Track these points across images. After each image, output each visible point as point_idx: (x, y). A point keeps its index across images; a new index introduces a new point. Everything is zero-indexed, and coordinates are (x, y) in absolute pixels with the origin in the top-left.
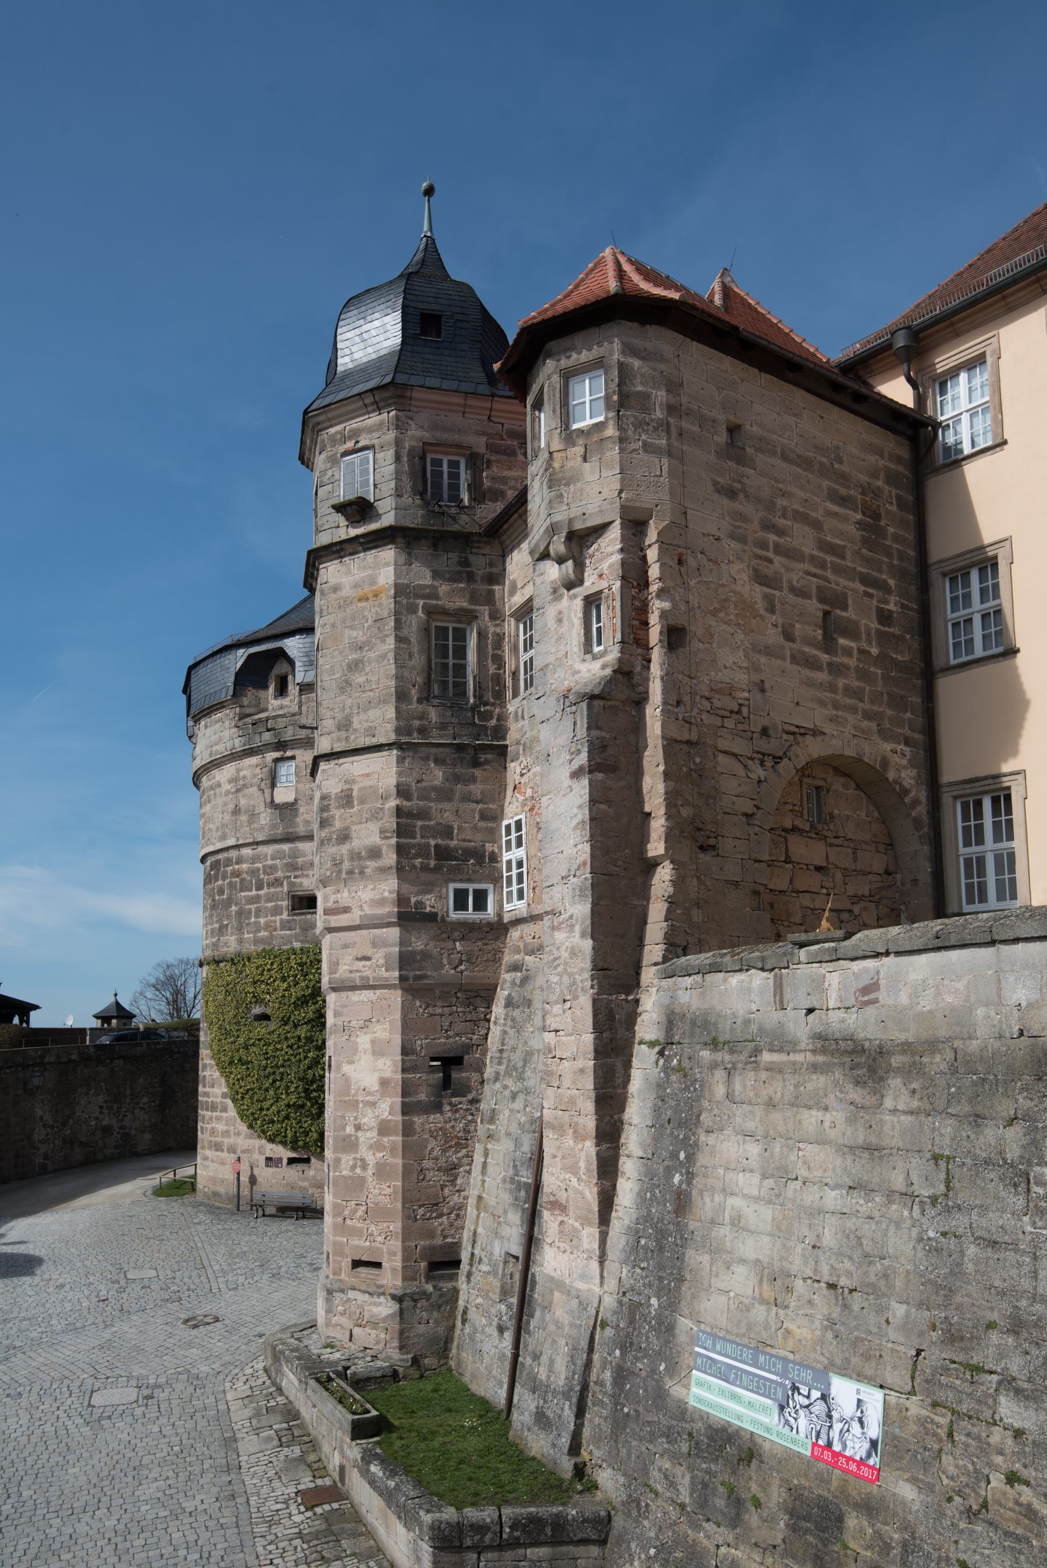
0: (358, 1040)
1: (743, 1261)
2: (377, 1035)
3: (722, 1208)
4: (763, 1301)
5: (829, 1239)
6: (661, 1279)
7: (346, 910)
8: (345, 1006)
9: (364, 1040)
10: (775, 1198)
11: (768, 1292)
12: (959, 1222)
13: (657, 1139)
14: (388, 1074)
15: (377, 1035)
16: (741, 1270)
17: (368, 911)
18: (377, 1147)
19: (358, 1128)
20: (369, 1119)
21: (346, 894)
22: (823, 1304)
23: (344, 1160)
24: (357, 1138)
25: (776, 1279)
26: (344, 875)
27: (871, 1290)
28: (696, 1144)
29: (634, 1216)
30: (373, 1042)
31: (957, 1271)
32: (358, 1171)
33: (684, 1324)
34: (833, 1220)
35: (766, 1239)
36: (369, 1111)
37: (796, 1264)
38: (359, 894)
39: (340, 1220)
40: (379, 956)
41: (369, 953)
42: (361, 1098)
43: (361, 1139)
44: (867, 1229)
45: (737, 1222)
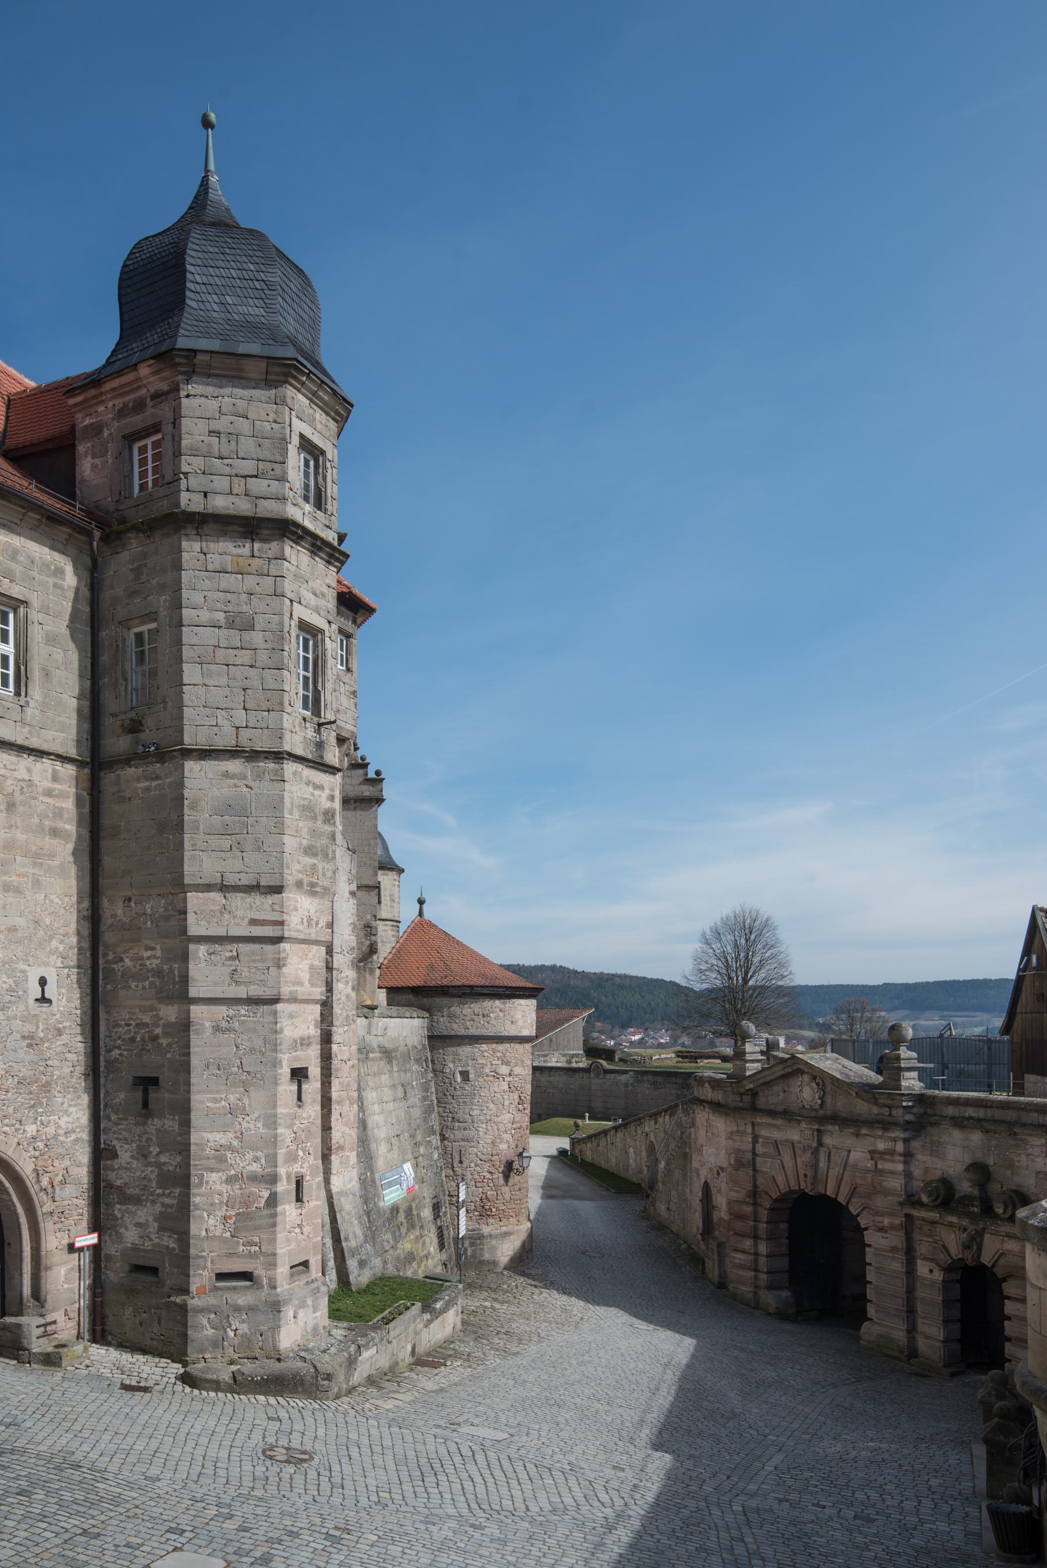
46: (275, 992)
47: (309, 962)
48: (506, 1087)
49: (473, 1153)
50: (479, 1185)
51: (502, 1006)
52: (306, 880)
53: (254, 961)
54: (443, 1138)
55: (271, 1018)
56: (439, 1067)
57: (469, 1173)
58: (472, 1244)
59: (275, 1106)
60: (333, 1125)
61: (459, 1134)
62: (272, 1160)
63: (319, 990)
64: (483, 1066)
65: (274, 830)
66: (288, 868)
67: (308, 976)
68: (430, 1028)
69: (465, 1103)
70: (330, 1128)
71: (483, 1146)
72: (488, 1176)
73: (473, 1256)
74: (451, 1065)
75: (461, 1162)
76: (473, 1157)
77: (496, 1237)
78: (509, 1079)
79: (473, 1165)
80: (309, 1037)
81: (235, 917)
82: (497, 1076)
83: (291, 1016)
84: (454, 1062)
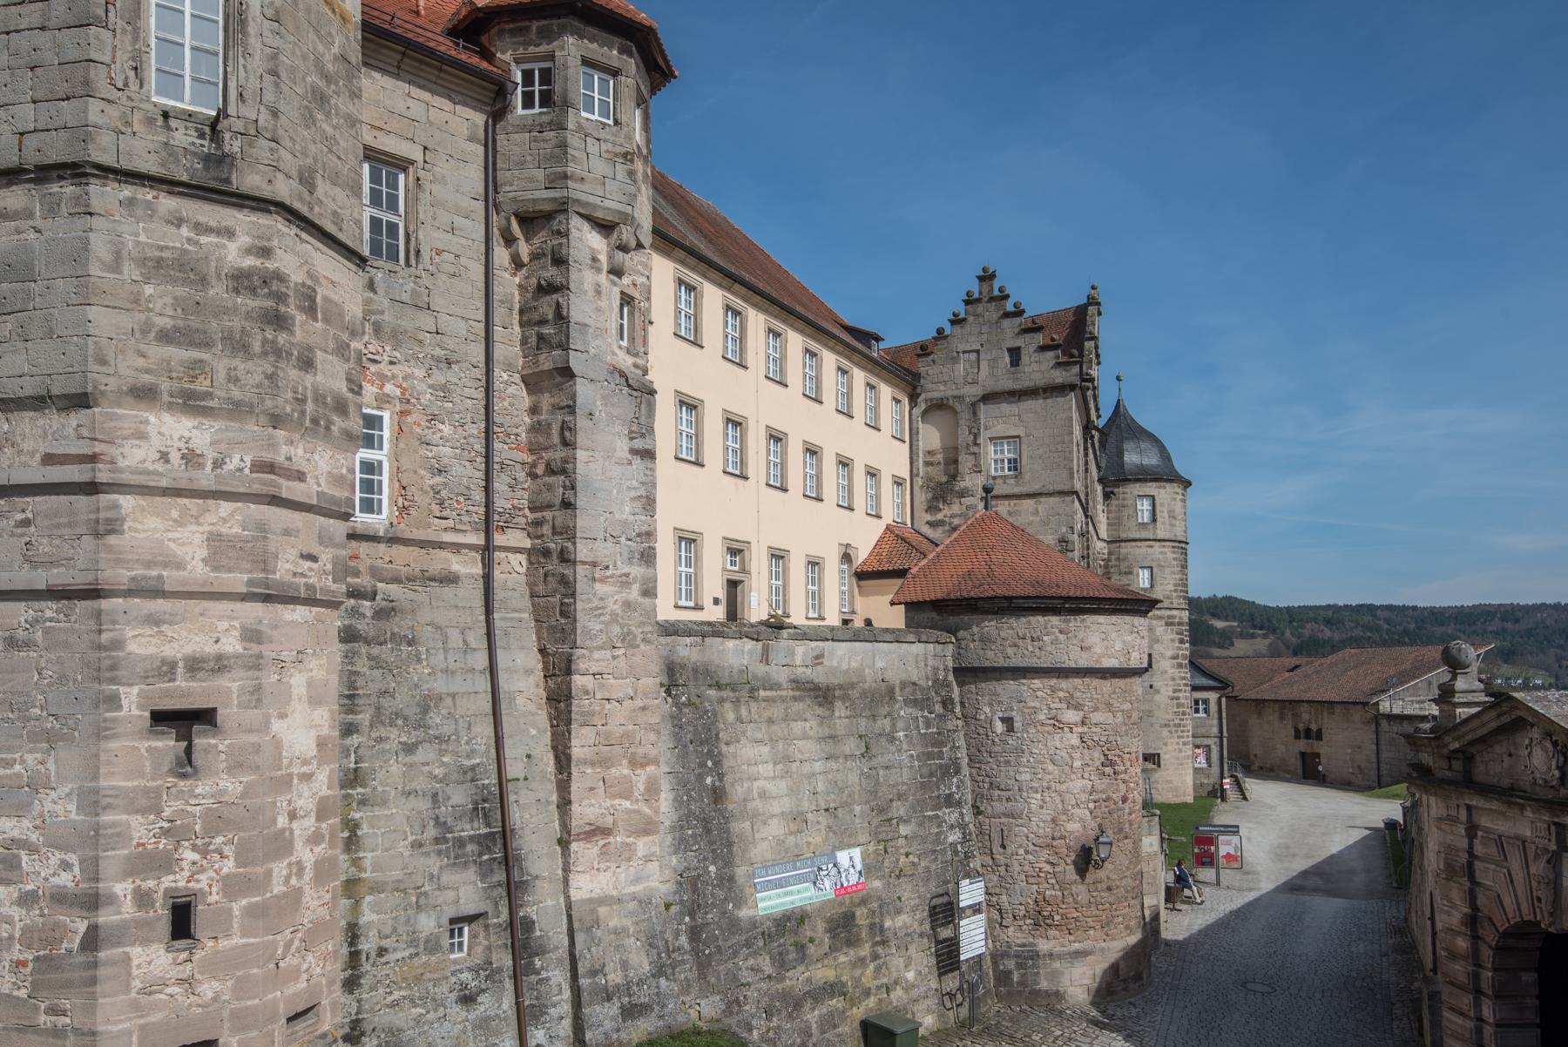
0: (292, 681)
1: (773, 816)
2: (314, 673)
3: (750, 790)
4: (791, 833)
5: (821, 787)
6: (714, 851)
7: (300, 476)
8: (276, 627)
9: (298, 682)
10: (786, 774)
11: (793, 827)
12: (875, 762)
13: (683, 756)
14: (326, 731)
15: (314, 673)
16: (775, 821)
17: (325, 488)
18: (315, 839)
19: (293, 816)
20: (304, 799)
21: (300, 451)
22: (824, 819)
23: (276, 870)
24: (291, 830)
25: (798, 819)
26: (307, 423)
27: (845, 804)
28: (720, 753)
29: (675, 818)
30: (310, 684)
31: (877, 783)
32: (293, 881)
33: (741, 872)
34: (820, 778)
35: (786, 799)
36: (305, 790)
37: (805, 805)
38: (316, 457)
39: (272, 966)
40: (326, 556)
41: (315, 549)
42: (296, 771)
43: (297, 832)
44: (839, 776)
45: (763, 795)
46: (90, 578)
47: (206, 528)
48: (1075, 741)
49: (1020, 833)
50: (1031, 880)
51: (1063, 626)
52: (165, 386)
53: (58, 526)
54: (977, 812)
55: (92, 624)
56: (971, 711)
57: (1016, 864)
58: (1020, 966)
59: (96, 776)
60: (573, 797)
61: (999, 807)
62: (92, 870)
63: (245, 577)
64: (1035, 710)
65: (75, 299)
66: (104, 362)
67: (203, 552)
68: (957, 657)
69: (1008, 763)
70: (570, 802)
71: (1038, 821)
72: (1048, 868)
73: (1022, 983)
74: (987, 709)
75: (1004, 847)
76: (1021, 840)
77: (1060, 957)
78: (1080, 730)
79: (1021, 851)
80: (219, 657)
81: (20, 452)
82: (1058, 724)
83: (153, 620)
84: (991, 705)
